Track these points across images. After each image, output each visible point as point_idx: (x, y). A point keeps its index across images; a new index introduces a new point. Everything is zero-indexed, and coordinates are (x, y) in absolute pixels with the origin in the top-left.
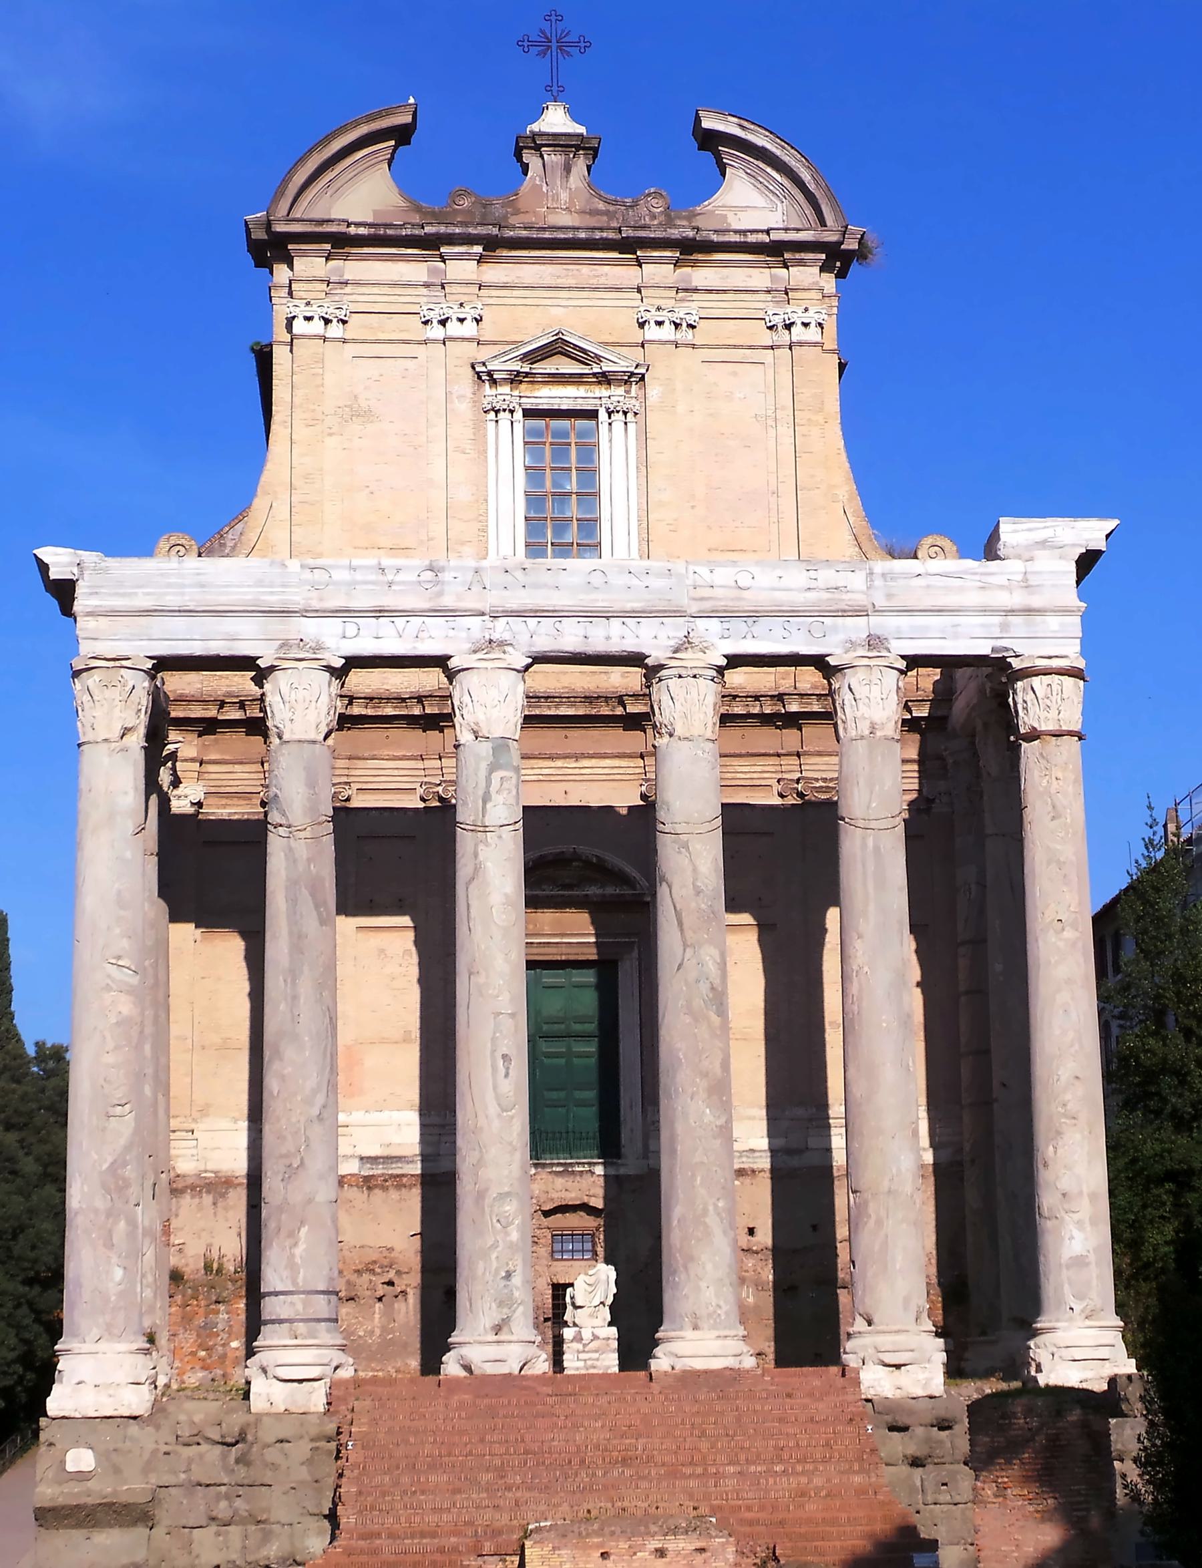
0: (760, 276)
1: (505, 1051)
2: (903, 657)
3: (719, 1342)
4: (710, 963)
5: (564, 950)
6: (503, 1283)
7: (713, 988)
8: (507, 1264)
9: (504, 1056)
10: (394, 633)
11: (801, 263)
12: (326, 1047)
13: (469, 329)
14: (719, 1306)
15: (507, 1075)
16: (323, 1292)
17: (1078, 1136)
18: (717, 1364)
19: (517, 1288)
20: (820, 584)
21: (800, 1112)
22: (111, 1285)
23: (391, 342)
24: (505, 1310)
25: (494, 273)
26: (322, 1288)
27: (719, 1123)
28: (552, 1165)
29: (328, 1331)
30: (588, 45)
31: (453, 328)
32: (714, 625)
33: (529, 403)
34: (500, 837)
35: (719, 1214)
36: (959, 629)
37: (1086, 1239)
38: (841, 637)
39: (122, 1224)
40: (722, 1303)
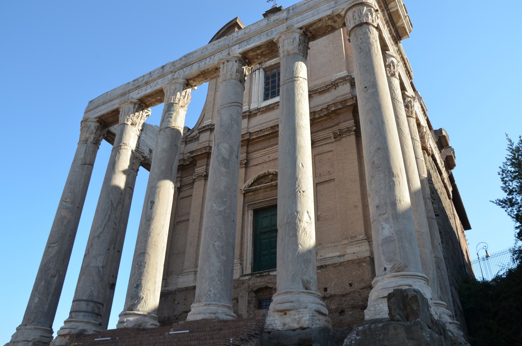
2: (301, 28)
4: (223, 150)
5: (266, 203)
6: (134, 289)
7: (223, 158)
8: (137, 281)
10: (149, 87)
14: (210, 290)
16: (84, 300)
17: (382, 175)
21: (346, 242)
22: (33, 304)
26: (84, 298)
27: (221, 209)
28: (256, 274)
29: (84, 316)
32: (237, 46)
33: (264, 67)
35: (215, 248)
37: (391, 227)
39: (43, 283)
40: (212, 289)
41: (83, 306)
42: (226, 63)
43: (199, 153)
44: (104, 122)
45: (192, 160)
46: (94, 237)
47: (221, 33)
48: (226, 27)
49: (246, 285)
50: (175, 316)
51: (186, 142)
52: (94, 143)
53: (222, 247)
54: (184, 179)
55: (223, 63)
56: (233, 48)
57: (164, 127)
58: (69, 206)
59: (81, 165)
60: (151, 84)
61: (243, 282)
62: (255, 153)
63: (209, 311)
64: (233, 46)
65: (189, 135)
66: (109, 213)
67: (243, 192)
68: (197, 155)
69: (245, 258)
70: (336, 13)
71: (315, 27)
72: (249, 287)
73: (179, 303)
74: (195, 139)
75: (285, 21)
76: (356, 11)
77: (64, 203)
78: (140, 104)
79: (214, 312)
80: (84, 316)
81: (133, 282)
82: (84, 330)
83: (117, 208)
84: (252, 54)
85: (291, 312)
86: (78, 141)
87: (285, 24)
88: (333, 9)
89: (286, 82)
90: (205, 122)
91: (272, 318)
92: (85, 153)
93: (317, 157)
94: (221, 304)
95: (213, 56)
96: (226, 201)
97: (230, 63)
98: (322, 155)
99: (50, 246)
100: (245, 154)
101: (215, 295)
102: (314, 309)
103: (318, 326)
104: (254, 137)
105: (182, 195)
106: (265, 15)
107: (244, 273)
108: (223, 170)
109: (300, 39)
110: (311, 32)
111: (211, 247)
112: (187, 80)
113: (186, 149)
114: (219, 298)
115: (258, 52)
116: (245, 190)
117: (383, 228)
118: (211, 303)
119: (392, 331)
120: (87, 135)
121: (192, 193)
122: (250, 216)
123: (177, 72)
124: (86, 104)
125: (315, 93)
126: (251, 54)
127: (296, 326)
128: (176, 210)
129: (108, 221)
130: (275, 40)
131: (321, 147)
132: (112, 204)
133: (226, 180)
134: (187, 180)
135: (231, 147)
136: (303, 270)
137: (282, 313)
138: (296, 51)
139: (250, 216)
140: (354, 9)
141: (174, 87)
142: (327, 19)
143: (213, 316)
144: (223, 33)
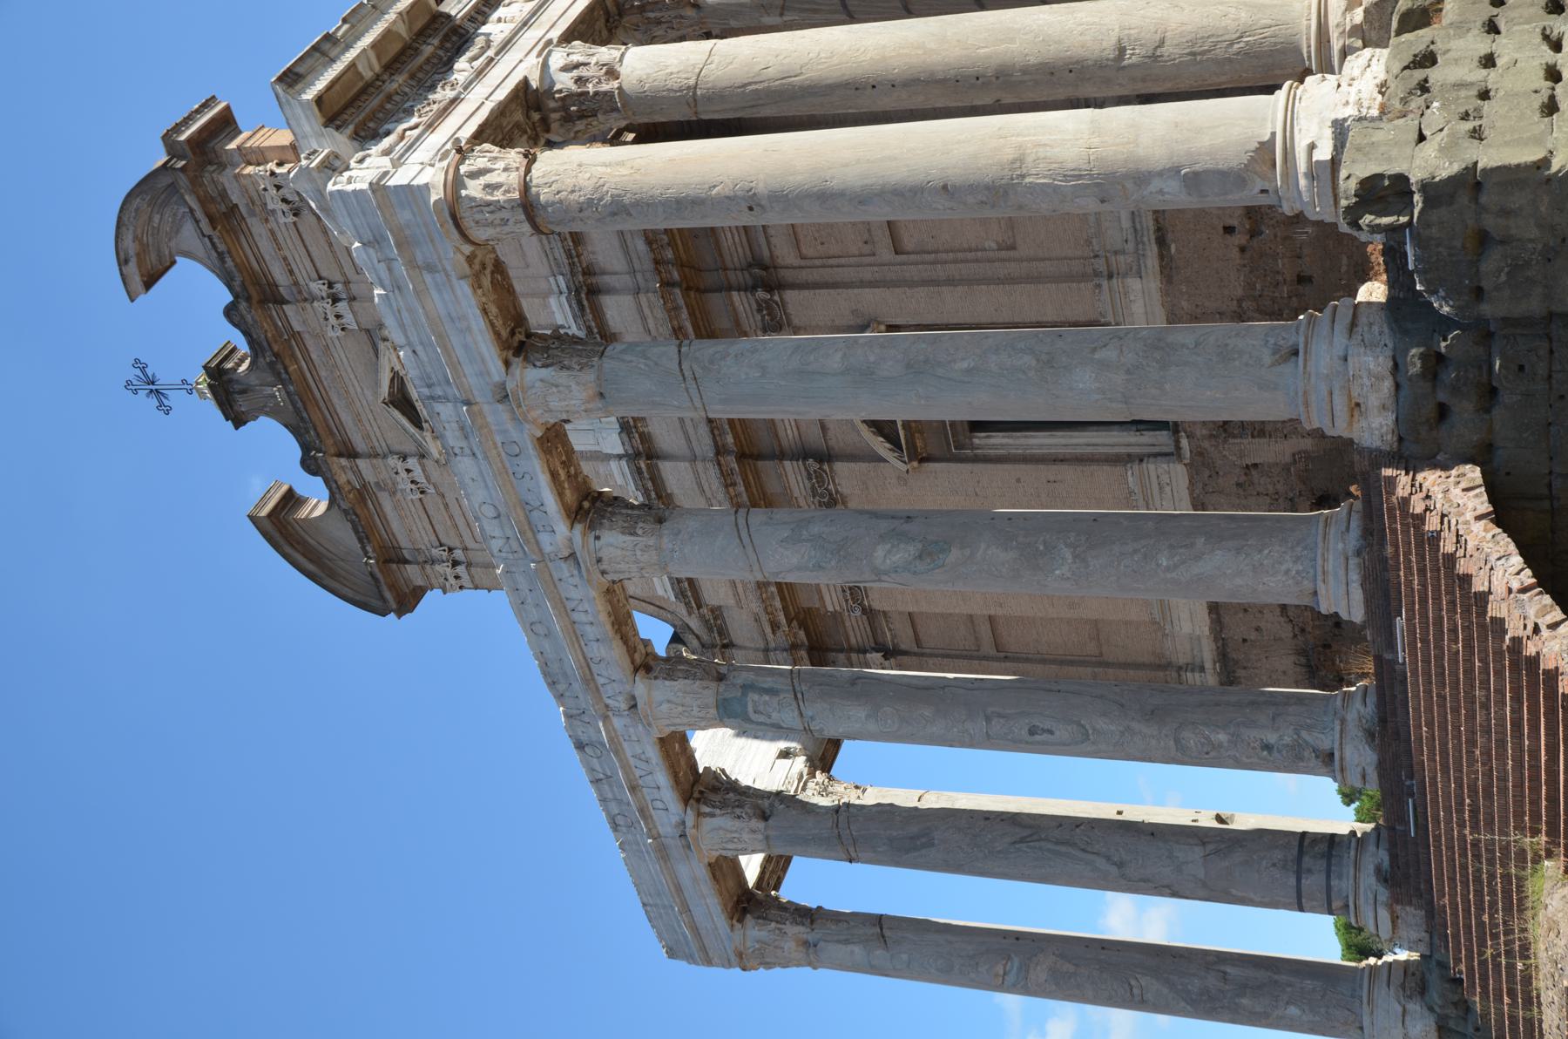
0: (257, 227)
1: (1024, 732)
2: (507, 364)
3: (1331, 578)
6: (1275, 754)
7: (920, 557)
9: (1032, 732)
11: (224, 194)
12: (1049, 850)
13: (412, 462)
14: (1287, 572)
15: (1051, 732)
16: (1299, 880)
18: (1355, 576)
19: (1281, 738)
20: (464, 444)
23: (451, 517)
24: (1306, 754)
25: (360, 446)
26: (1293, 881)
27: (1069, 556)
29: (1340, 877)
30: (137, 361)
31: (418, 474)
32: (544, 538)
34: (812, 718)
35: (1176, 566)
36: (454, 314)
38: (510, 426)
39: (1245, 1001)
40: (1284, 568)
41: (1314, 882)
42: (604, 566)
43: (778, 604)
44: (738, 902)
45: (795, 623)
46: (1123, 876)
47: (311, 567)
48: (288, 549)
49: (1206, 444)
50: (1295, 636)
51: (725, 646)
52: (812, 922)
53: (1171, 547)
54: (853, 641)
55: (603, 573)
56: (548, 549)
57: (798, 720)
58: (1016, 964)
59: (886, 948)
60: (638, 773)
61: (1199, 453)
62: (781, 434)
63: (1342, 572)
64: (540, 550)
65: (698, 637)
66: (1050, 846)
67: (915, 464)
68: (785, 608)
69: (1123, 450)
70: (466, 266)
71: (499, 323)
72: (1211, 436)
73: (1258, 629)
74: (715, 619)
75: (475, 408)
76: (478, 217)
77: (1011, 978)
78: (698, 800)
79: (1342, 560)
80: (1340, 877)
81: (1255, 760)
82: (1378, 870)
83: (1031, 827)
84: (568, 492)
85: (1355, 394)
86: (809, 969)
87: (486, 408)
88: (454, 280)
89: (698, 404)
90: (660, 592)
91: (1366, 435)
92: (847, 942)
93: (804, 251)
94: (1320, 545)
95: (570, 605)
96: (1045, 543)
97: (604, 554)
98: (801, 237)
99: (1137, 999)
100: (787, 464)
101: (1297, 560)
102: (1345, 341)
103: (1386, 330)
104: (730, 439)
105: (906, 643)
106: (239, 422)
107: (1171, 449)
108: (955, 554)
109: (545, 366)
110: (512, 333)
111: (1174, 575)
112: (636, 670)
113: (748, 644)
114: (1305, 548)
115: (563, 476)
116: (910, 460)
117: (1161, 192)
118: (1319, 569)
119: (1434, 231)
120: (790, 946)
121: (901, 613)
122: (992, 441)
123: (609, 701)
124: (681, 965)
125: (578, 256)
126: (570, 496)
127: (1387, 384)
128: (957, 657)
129: (1074, 845)
130: (539, 434)
131: (774, 241)
132: (1022, 840)
133: (983, 546)
134: (855, 628)
135: (883, 538)
136: (1247, 365)
137: (1356, 413)
138: (589, 376)
139: (992, 441)
140: (468, 223)
141: (665, 707)
142: (480, 292)
143: (1353, 562)
144: (310, 560)
